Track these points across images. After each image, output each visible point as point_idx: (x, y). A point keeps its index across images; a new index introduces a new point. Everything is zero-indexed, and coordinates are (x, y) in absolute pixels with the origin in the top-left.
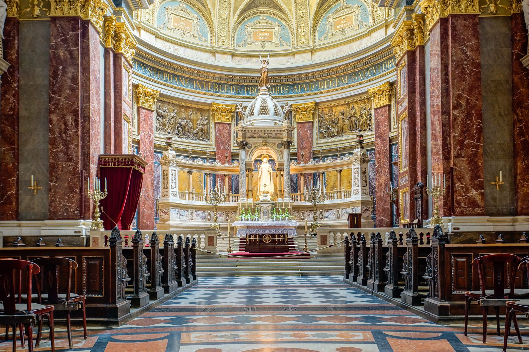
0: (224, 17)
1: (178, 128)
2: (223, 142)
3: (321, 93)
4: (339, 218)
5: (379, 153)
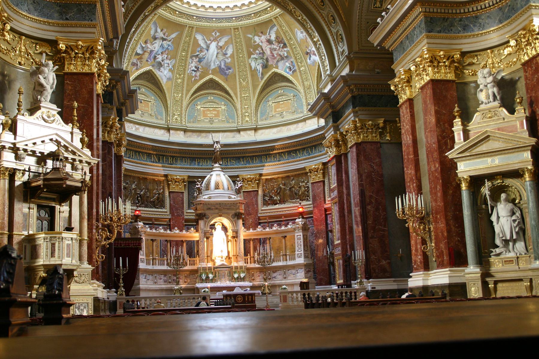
0: (178, 99)
1: (138, 197)
2: (177, 209)
3: (264, 166)
4: (285, 278)
5: (317, 221)
